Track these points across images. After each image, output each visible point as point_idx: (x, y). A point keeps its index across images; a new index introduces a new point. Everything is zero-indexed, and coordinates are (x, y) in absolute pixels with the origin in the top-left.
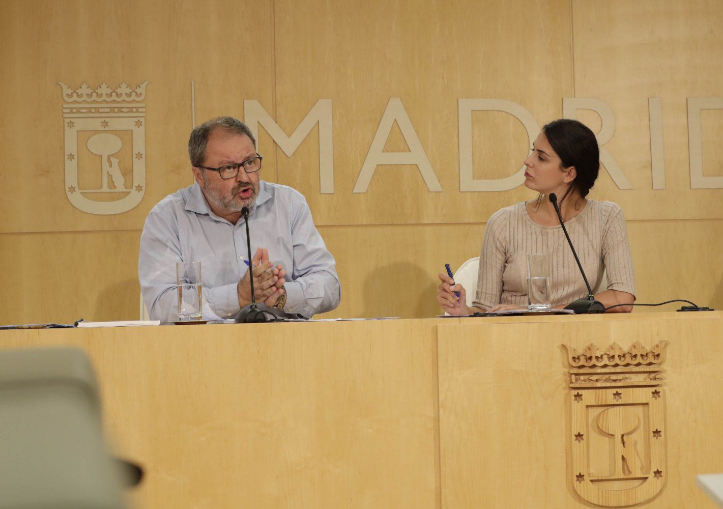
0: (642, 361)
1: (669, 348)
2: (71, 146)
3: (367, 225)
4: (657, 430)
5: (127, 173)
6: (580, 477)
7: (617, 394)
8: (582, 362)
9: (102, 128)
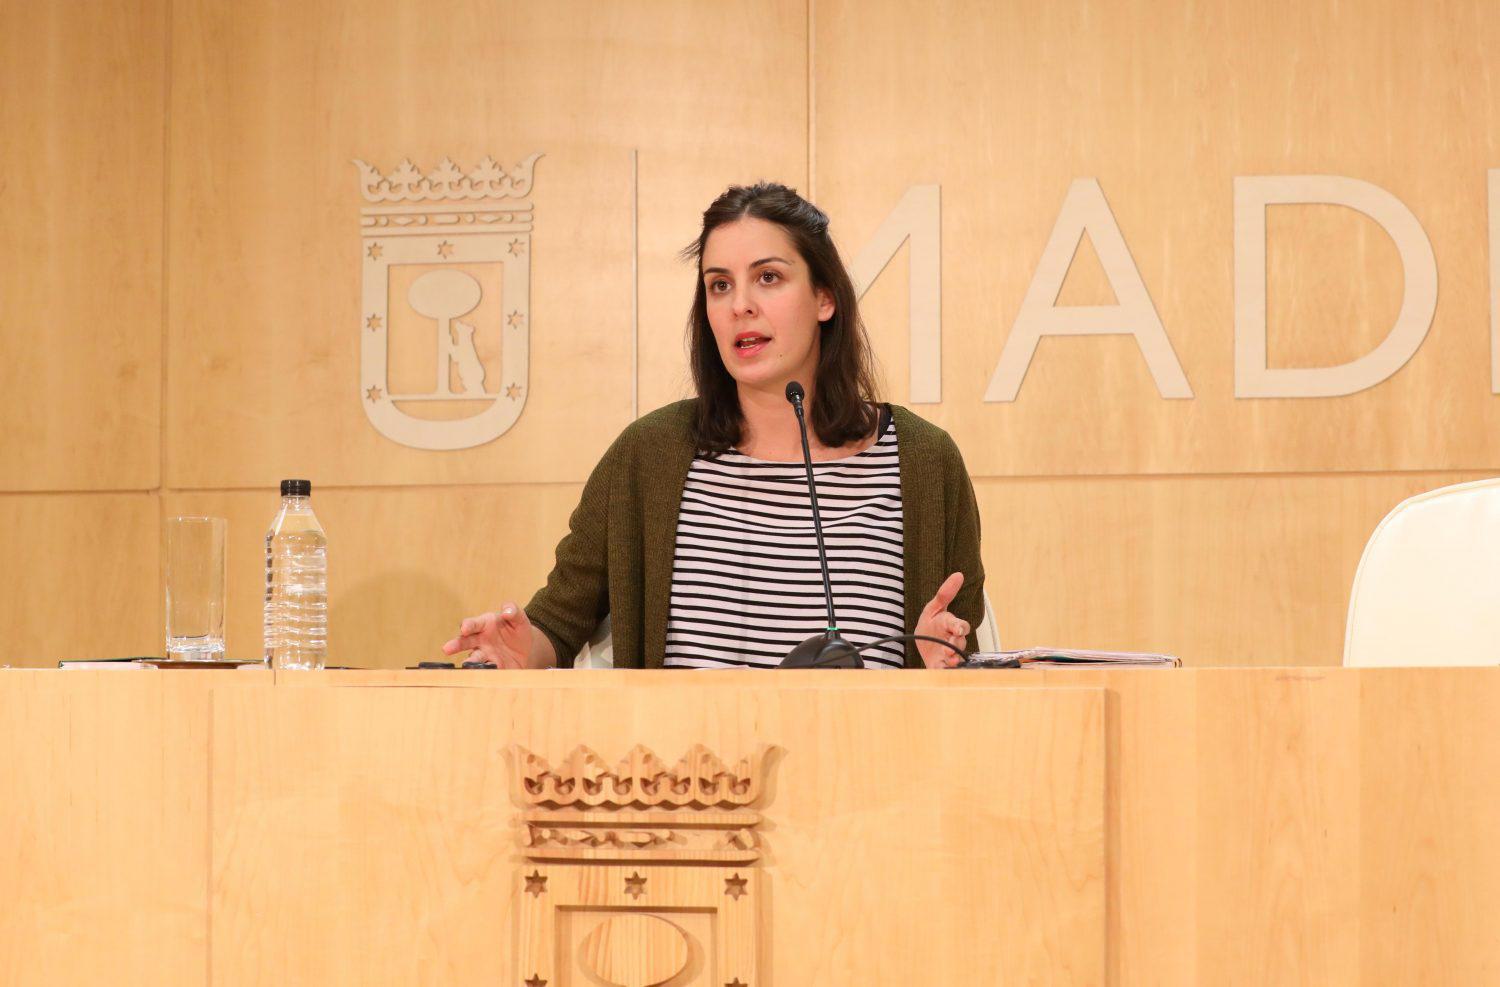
0: (703, 796)
1: (783, 771)
2: (373, 303)
3: (1015, 478)
7: (635, 882)
8: (548, 792)
9: (440, 259)
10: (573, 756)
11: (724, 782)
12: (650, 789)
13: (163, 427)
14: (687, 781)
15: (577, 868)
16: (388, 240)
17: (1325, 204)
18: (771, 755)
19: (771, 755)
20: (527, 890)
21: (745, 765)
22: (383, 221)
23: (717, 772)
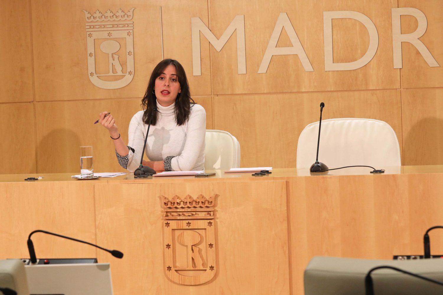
1: (219, 199)
4: (211, 244)
5: (123, 64)
6: (169, 268)
8: (169, 205)
10: (174, 197)
11: (207, 202)
12: (191, 204)
13: (34, 83)
14: (199, 202)
15: (176, 221)
16: (93, 32)
17: (348, 18)
18: (217, 196)
19: (217, 196)
20: (166, 226)
21: (211, 199)
22: (92, 27)
23: (205, 200)
